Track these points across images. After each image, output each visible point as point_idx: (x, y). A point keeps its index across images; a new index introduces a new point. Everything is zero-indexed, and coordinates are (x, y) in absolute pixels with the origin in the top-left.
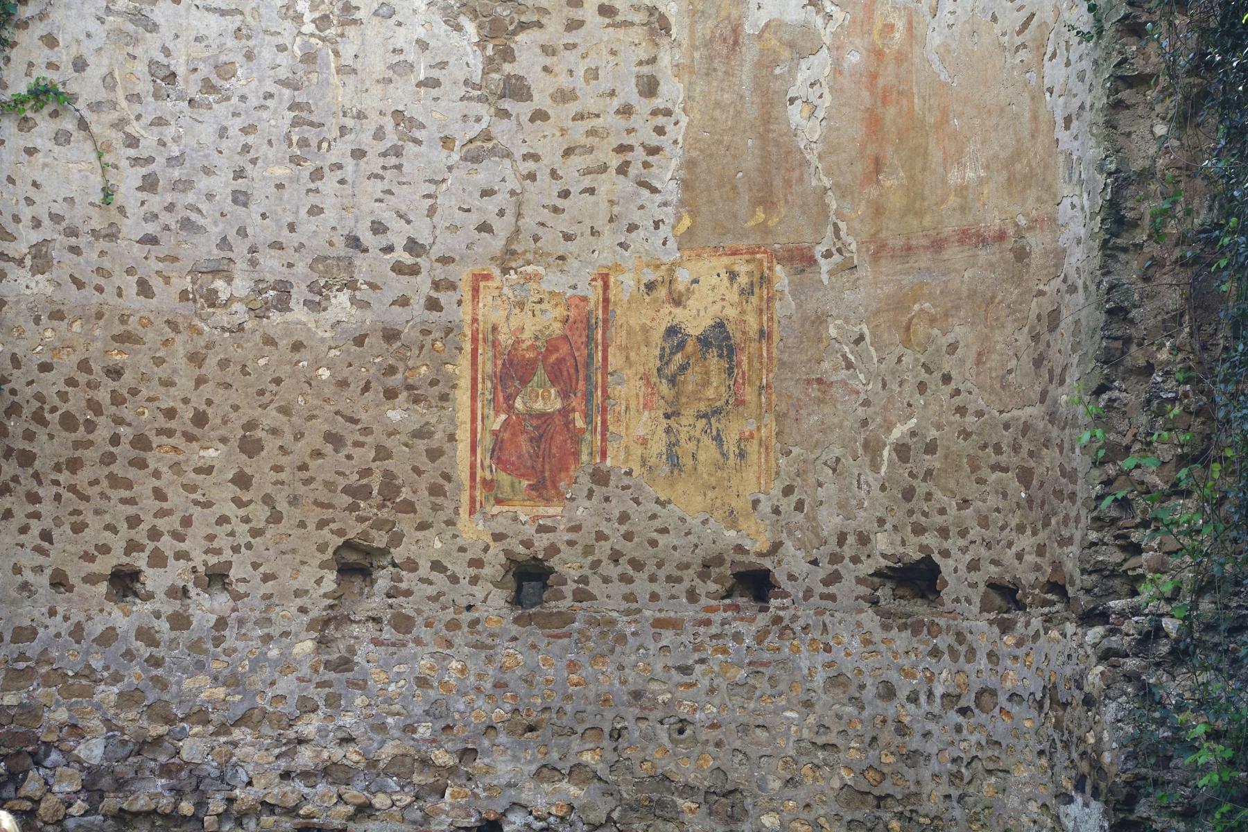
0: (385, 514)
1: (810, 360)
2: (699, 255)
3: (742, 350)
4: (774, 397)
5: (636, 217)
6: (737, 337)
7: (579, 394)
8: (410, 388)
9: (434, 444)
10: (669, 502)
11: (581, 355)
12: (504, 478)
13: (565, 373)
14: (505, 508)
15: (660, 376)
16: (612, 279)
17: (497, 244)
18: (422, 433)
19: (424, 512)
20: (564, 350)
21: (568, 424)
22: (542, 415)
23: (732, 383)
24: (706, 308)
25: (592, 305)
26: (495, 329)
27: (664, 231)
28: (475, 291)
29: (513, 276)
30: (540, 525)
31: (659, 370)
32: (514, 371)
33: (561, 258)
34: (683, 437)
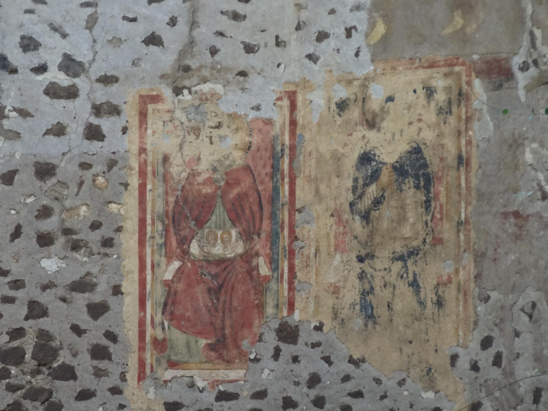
0: (40, 381)
1: (507, 190)
2: (393, 68)
3: (440, 179)
4: (473, 234)
5: (326, 23)
6: (435, 166)
7: (263, 235)
8: (67, 232)
9: (96, 297)
10: (363, 360)
11: (265, 188)
12: (178, 337)
13: (247, 211)
14: (179, 373)
15: (352, 212)
16: (300, 98)
17: (165, 58)
18: (82, 285)
19: (86, 380)
20: (246, 183)
21: (252, 272)
22: (221, 261)
23: (429, 218)
24: (402, 131)
25: (277, 129)
26: (166, 159)
27: (357, 39)
28: (143, 115)
29: (186, 96)
30: (220, 392)
31: (352, 205)
32: (188, 212)
33: (243, 74)
34: (378, 283)
